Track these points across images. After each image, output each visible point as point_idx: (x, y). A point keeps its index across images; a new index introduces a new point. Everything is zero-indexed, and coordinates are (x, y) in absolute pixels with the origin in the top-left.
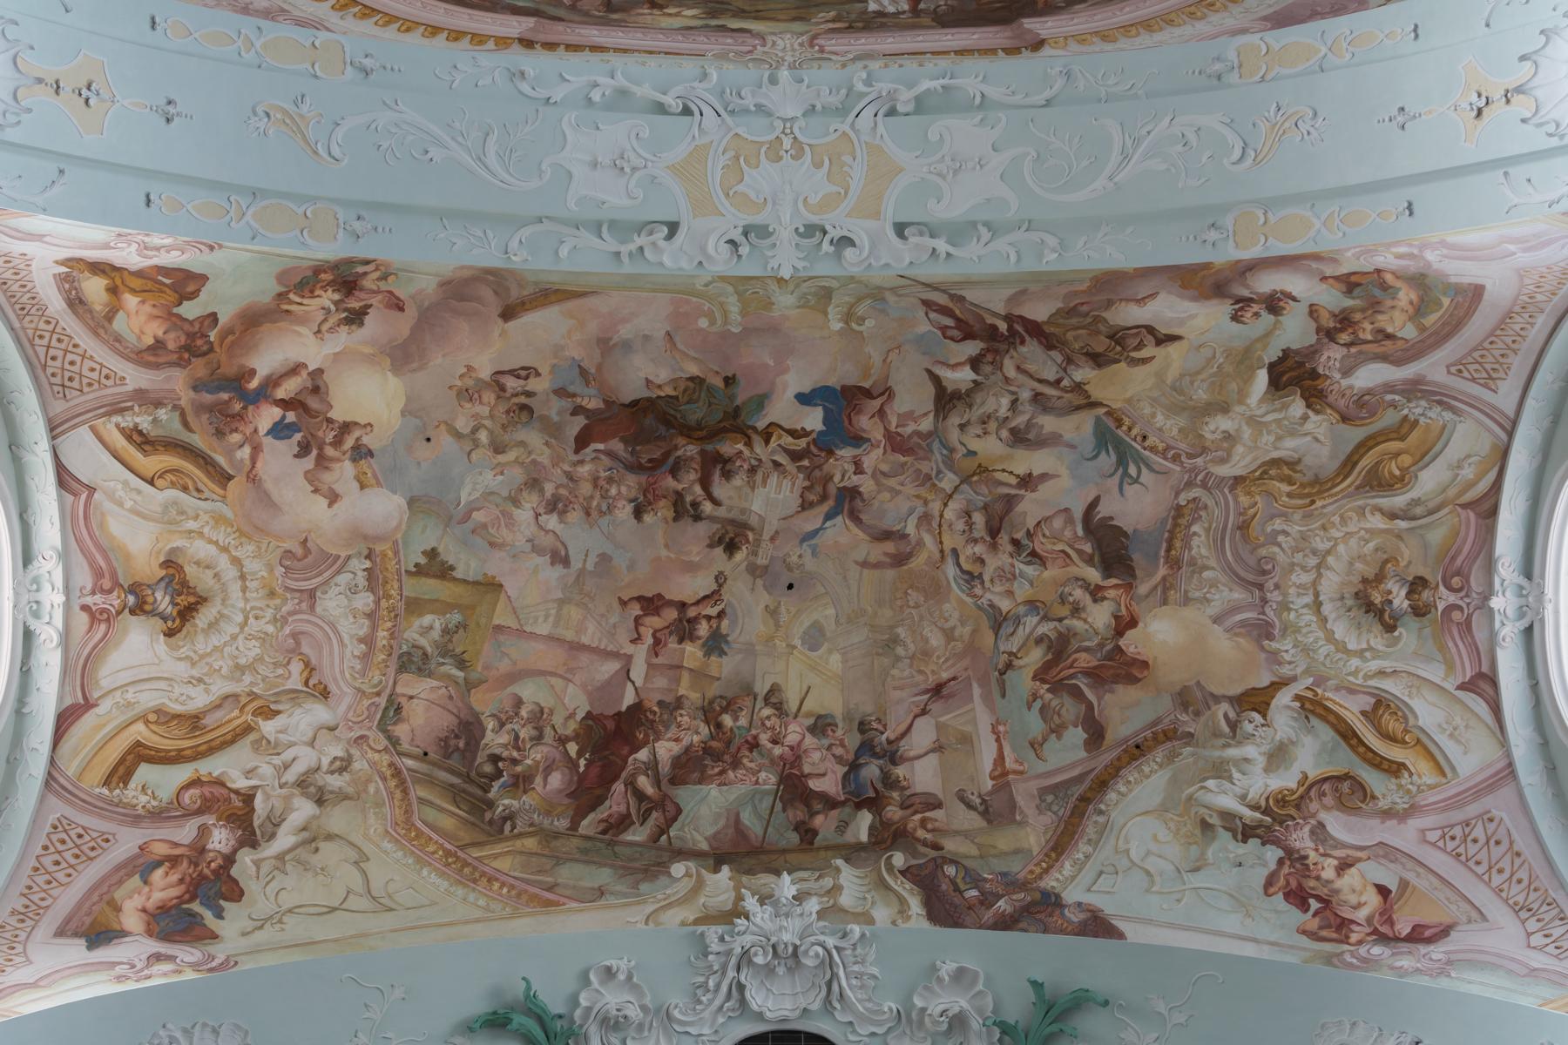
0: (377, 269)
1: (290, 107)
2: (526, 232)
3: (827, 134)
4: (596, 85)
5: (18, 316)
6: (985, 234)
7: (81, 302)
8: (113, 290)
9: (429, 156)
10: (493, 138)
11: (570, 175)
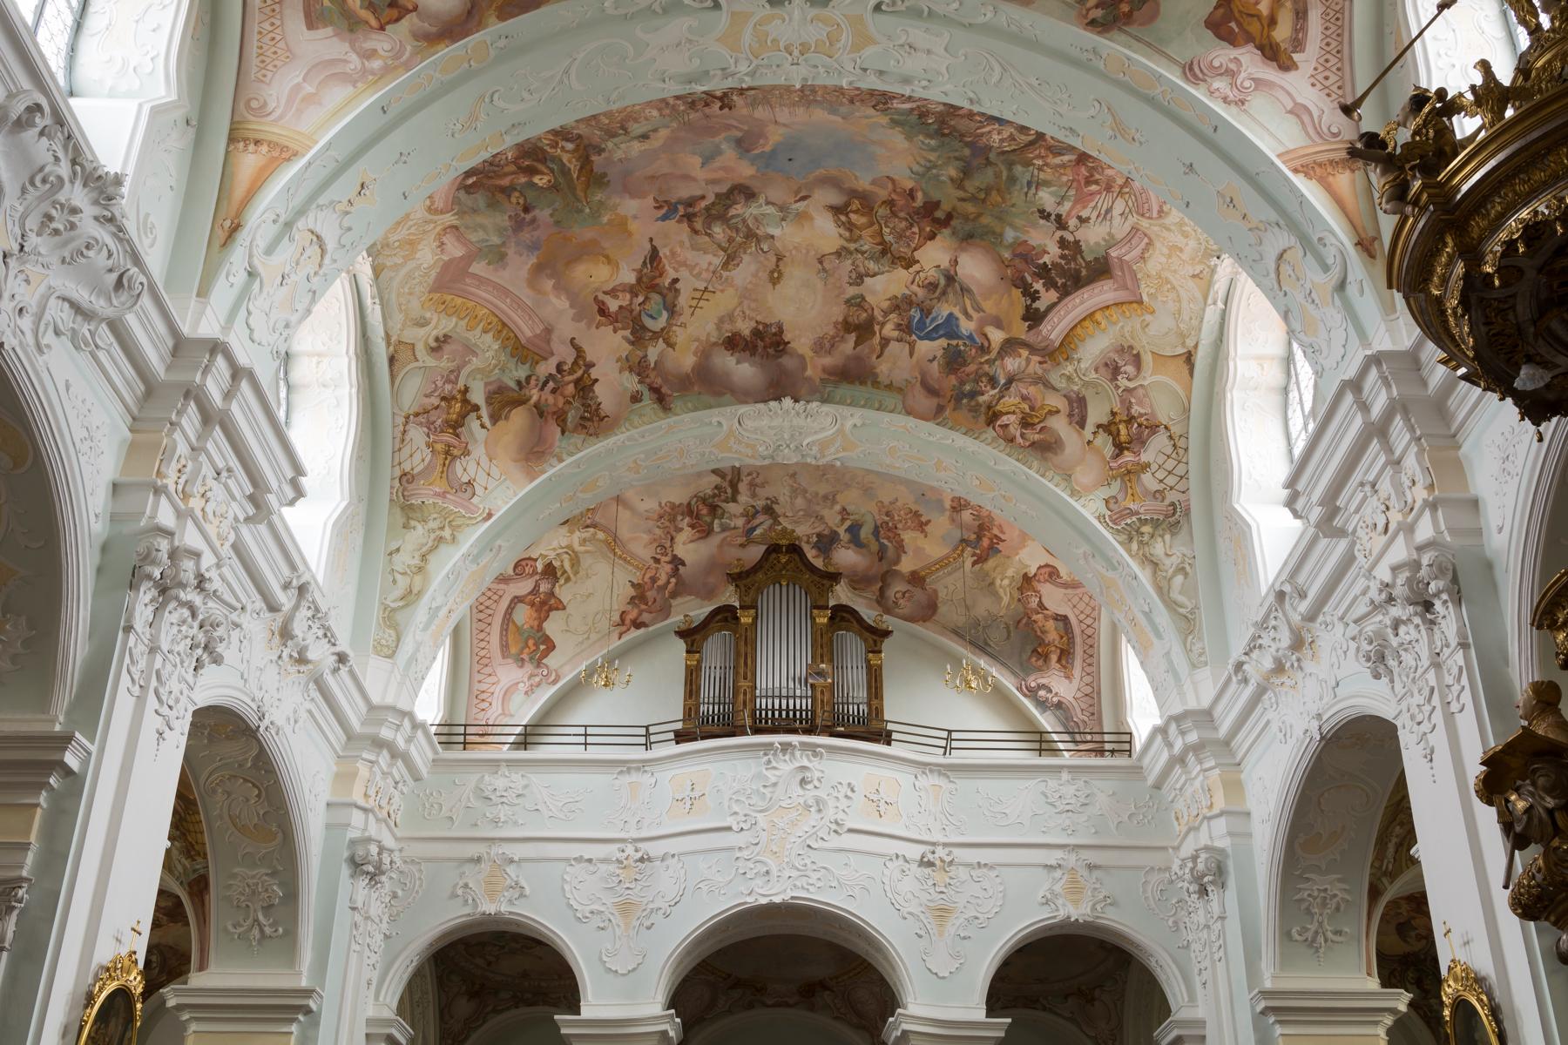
0: (1088, 10)
1: (1118, 135)
2: (981, 20)
3: (768, 57)
4: (924, 88)
5: (1343, 14)
6: (656, 7)
7: (1297, 14)
8: (1272, 21)
9: (1038, 82)
10: (994, 80)
11: (946, 49)
